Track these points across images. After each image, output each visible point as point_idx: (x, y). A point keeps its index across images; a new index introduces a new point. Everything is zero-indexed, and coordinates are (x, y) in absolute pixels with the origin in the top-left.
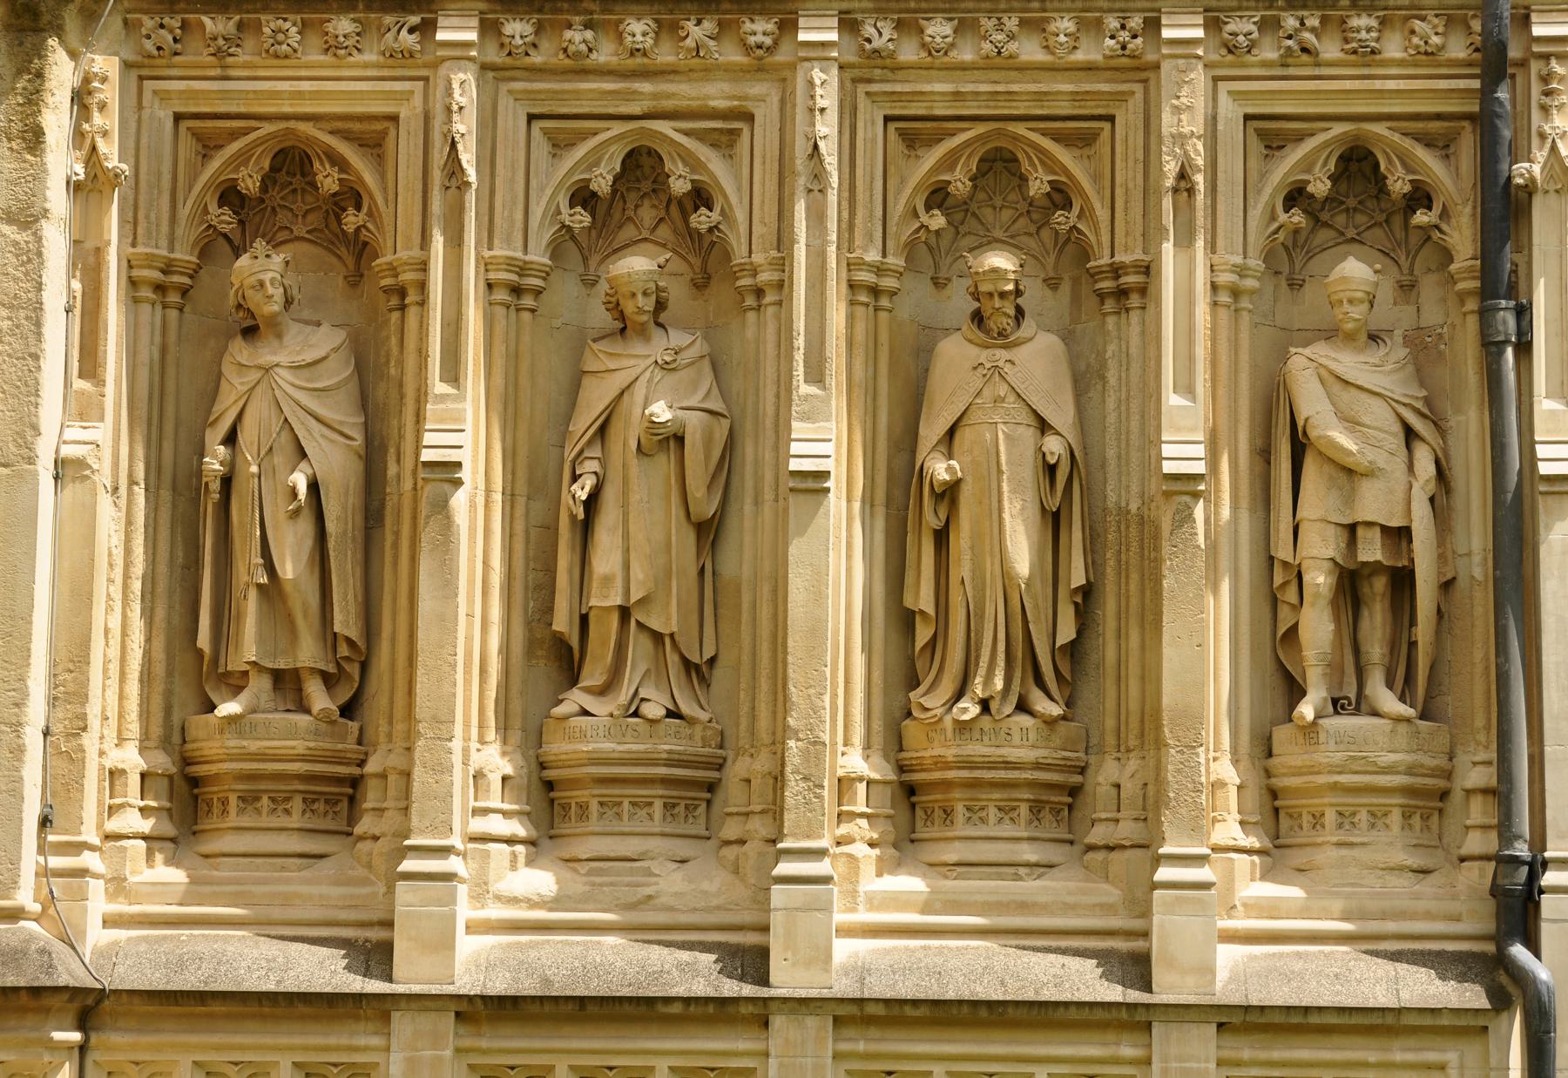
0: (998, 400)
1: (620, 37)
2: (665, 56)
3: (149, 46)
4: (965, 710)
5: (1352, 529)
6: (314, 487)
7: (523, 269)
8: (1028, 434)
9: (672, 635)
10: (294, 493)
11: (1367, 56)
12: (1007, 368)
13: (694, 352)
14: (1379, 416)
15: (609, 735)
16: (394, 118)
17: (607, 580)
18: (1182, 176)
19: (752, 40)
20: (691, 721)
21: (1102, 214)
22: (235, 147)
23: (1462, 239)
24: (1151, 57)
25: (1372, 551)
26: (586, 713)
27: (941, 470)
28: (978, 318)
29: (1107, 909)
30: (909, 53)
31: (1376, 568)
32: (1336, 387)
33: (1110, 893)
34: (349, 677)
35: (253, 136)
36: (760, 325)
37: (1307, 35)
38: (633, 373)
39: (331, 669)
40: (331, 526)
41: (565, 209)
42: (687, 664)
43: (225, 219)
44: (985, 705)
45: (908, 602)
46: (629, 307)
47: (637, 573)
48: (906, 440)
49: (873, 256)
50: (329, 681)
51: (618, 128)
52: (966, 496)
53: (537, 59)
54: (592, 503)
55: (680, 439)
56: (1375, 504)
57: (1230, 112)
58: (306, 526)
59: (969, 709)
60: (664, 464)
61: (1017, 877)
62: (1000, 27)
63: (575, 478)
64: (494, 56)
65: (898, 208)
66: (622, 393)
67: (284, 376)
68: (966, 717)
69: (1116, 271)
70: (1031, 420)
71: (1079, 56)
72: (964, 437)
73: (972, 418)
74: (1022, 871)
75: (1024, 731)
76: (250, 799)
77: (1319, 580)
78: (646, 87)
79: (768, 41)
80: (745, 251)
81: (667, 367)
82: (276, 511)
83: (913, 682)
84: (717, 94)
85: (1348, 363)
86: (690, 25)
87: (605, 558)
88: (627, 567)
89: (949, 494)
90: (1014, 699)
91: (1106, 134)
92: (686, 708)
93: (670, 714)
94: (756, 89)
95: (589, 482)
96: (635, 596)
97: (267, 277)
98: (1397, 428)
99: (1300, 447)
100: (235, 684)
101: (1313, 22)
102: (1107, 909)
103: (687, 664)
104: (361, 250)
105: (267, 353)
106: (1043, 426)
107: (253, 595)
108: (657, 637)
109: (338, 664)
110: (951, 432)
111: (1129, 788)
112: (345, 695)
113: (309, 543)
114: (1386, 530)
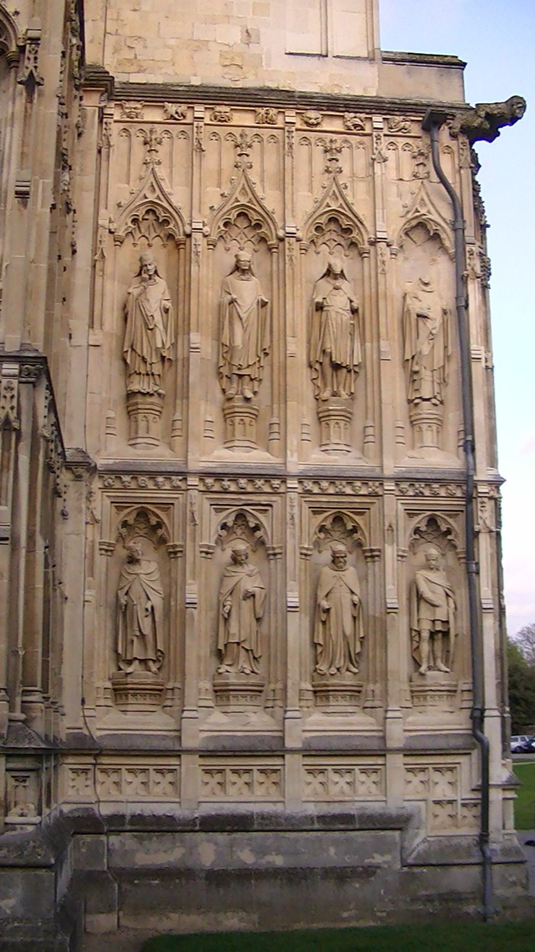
0: (341, 586)
1: (237, 484)
2: (250, 489)
3: (106, 484)
4: (333, 671)
5: (433, 621)
6: (152, 608)
7: (209, 547)
8: (349, 595)
9: (252, 650)
10: (147, 610)
11: (436, 495)
12: (343, 577)
13: (255, 571)
14: (440, 591)
15: (236, 678)
16: (173, 504)
17: (234, 635)
18: (390, 526)
19: (274, 486)
20: (257, 674)
21: (367, 534)
22: (128, 510)
23: (461, 543)
24: (381, 493)
25: (439, 627)
26: (228, 671)
27: (325, 604)
28: (333, 562)
29: (372, 724)
30: (316, 490)
31: (439, 631)
32: (430, 583)
33: (372, 720)
34: (160, 661)
35: (133, 508)
36: (276, 563)
37: (421, 489)
38: (240, 577)
39: (155, 659)
40: (157, 619)
41: (220, 531)
42: (255, 658)
43: (124, 531)
44: (338, 669)
45: (316, 641)
46: (239, 558)
47: (242, 633)
48: (315, 597)
49: (306, 546)
50: (154, 661)
51: (235, 508)
52: (332, 611)
53: (214, 489)
54: (229, 614)
55: (254, 596)
56: (441, 614)
57: (401, 508)
58: (150, 619)
59: (333, 670)
60: (249, 602)
61: (347, 716)
62: (341, 485)
63: (224, 606)
64: (202, 488)
65: (312, 531)
66: (237, 584)
67: (143, 577)
68: (333, 673)
69: (372, 551)
70: (349, 591)
71: (361, 493)
72: (331, 596)
73: (335, 590)
74: (349, 714)
75: (348, 676)
76: (134, 695)
77: (425, 635)
78: (243, 497)
79: (278, 486)
80: (270, 543)
81: (250, 576)
82: (141, 614)
83: (317, 663)
84: (263, 499)
85: (432, 576)
86: (257, 481)
87: (234, 628)
88: (239, 631)
89: (327, 611)
90: (345, 668)
91: (367, 514)
92: (256, 671)
93: (253, 672)
94: (274, 498)
95: (228, 607)
96: (242, 639)
97: (138, 549)
98: (444, 594)
99: (420, 597)
100: (129, 662)
101: (423, 486)
102: (372, 724)
103: (255, 658)
104: (163, 541)
105: (136, 569)
106: (352, 592)
107: (135, 639)
108: (247, 650)
109: (157, 658)
110: (327, 595)
111: (377, 692)
112: (158, 665)
113: (151, 623)
114: (443, 622)
